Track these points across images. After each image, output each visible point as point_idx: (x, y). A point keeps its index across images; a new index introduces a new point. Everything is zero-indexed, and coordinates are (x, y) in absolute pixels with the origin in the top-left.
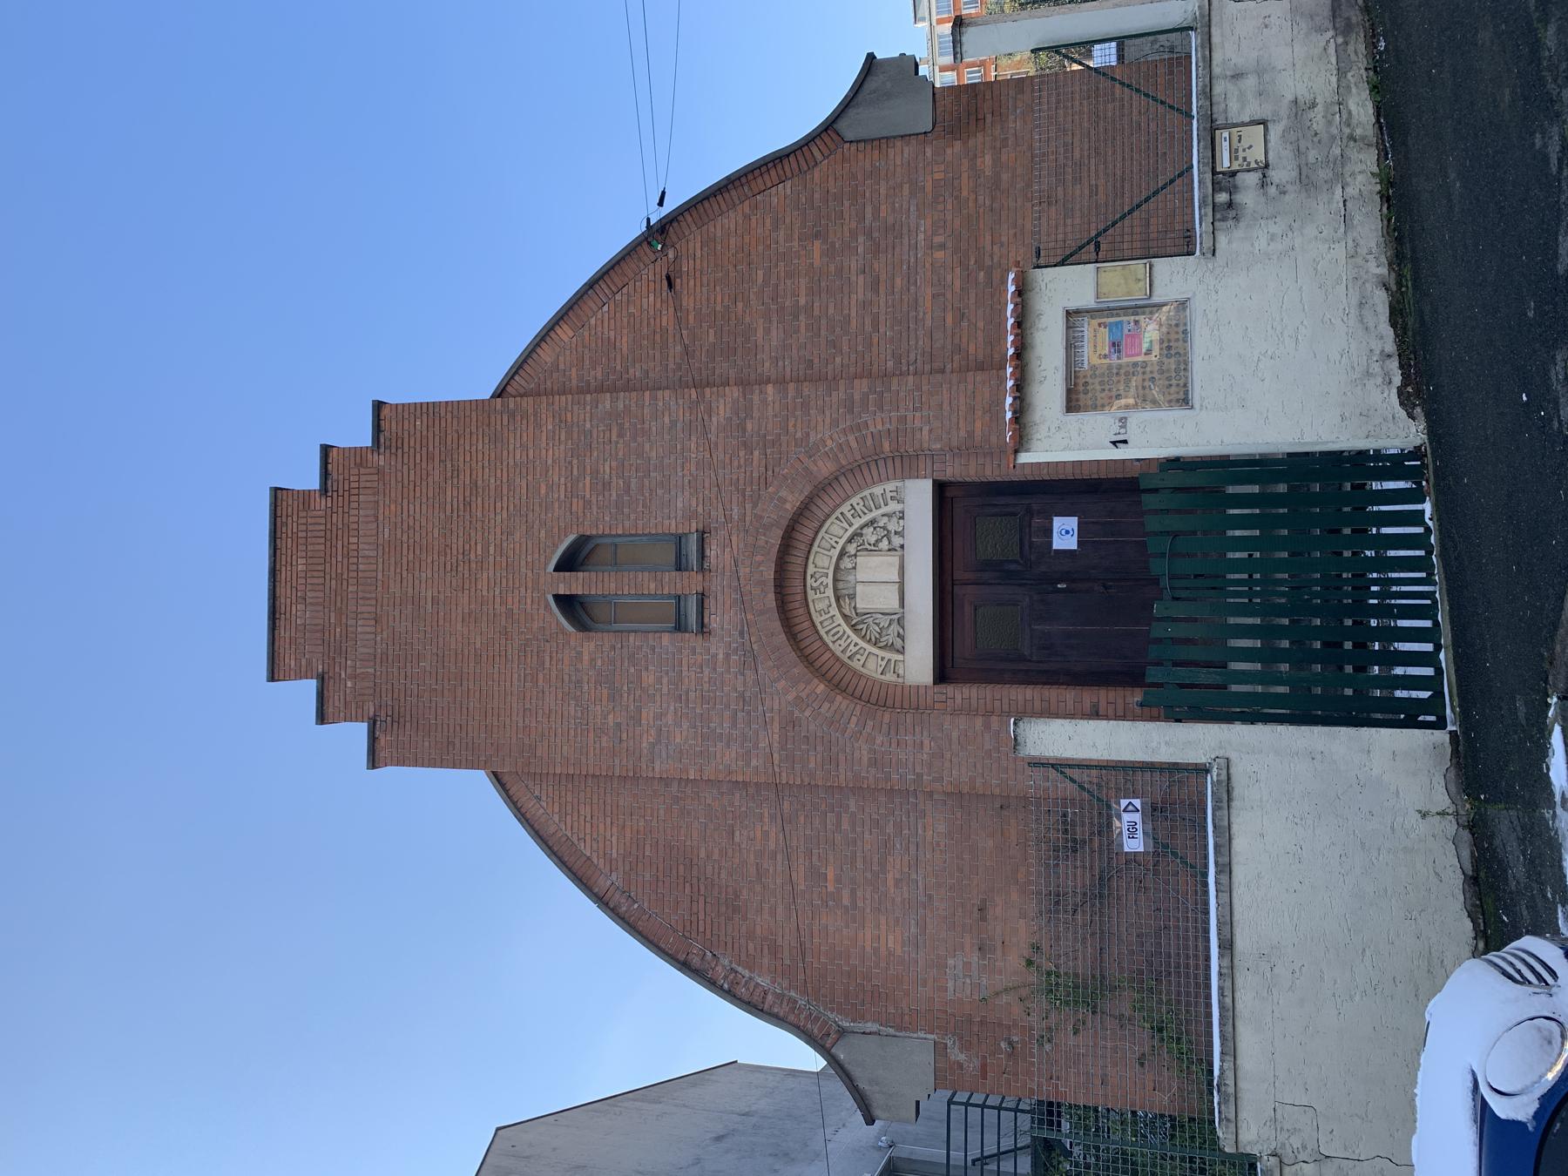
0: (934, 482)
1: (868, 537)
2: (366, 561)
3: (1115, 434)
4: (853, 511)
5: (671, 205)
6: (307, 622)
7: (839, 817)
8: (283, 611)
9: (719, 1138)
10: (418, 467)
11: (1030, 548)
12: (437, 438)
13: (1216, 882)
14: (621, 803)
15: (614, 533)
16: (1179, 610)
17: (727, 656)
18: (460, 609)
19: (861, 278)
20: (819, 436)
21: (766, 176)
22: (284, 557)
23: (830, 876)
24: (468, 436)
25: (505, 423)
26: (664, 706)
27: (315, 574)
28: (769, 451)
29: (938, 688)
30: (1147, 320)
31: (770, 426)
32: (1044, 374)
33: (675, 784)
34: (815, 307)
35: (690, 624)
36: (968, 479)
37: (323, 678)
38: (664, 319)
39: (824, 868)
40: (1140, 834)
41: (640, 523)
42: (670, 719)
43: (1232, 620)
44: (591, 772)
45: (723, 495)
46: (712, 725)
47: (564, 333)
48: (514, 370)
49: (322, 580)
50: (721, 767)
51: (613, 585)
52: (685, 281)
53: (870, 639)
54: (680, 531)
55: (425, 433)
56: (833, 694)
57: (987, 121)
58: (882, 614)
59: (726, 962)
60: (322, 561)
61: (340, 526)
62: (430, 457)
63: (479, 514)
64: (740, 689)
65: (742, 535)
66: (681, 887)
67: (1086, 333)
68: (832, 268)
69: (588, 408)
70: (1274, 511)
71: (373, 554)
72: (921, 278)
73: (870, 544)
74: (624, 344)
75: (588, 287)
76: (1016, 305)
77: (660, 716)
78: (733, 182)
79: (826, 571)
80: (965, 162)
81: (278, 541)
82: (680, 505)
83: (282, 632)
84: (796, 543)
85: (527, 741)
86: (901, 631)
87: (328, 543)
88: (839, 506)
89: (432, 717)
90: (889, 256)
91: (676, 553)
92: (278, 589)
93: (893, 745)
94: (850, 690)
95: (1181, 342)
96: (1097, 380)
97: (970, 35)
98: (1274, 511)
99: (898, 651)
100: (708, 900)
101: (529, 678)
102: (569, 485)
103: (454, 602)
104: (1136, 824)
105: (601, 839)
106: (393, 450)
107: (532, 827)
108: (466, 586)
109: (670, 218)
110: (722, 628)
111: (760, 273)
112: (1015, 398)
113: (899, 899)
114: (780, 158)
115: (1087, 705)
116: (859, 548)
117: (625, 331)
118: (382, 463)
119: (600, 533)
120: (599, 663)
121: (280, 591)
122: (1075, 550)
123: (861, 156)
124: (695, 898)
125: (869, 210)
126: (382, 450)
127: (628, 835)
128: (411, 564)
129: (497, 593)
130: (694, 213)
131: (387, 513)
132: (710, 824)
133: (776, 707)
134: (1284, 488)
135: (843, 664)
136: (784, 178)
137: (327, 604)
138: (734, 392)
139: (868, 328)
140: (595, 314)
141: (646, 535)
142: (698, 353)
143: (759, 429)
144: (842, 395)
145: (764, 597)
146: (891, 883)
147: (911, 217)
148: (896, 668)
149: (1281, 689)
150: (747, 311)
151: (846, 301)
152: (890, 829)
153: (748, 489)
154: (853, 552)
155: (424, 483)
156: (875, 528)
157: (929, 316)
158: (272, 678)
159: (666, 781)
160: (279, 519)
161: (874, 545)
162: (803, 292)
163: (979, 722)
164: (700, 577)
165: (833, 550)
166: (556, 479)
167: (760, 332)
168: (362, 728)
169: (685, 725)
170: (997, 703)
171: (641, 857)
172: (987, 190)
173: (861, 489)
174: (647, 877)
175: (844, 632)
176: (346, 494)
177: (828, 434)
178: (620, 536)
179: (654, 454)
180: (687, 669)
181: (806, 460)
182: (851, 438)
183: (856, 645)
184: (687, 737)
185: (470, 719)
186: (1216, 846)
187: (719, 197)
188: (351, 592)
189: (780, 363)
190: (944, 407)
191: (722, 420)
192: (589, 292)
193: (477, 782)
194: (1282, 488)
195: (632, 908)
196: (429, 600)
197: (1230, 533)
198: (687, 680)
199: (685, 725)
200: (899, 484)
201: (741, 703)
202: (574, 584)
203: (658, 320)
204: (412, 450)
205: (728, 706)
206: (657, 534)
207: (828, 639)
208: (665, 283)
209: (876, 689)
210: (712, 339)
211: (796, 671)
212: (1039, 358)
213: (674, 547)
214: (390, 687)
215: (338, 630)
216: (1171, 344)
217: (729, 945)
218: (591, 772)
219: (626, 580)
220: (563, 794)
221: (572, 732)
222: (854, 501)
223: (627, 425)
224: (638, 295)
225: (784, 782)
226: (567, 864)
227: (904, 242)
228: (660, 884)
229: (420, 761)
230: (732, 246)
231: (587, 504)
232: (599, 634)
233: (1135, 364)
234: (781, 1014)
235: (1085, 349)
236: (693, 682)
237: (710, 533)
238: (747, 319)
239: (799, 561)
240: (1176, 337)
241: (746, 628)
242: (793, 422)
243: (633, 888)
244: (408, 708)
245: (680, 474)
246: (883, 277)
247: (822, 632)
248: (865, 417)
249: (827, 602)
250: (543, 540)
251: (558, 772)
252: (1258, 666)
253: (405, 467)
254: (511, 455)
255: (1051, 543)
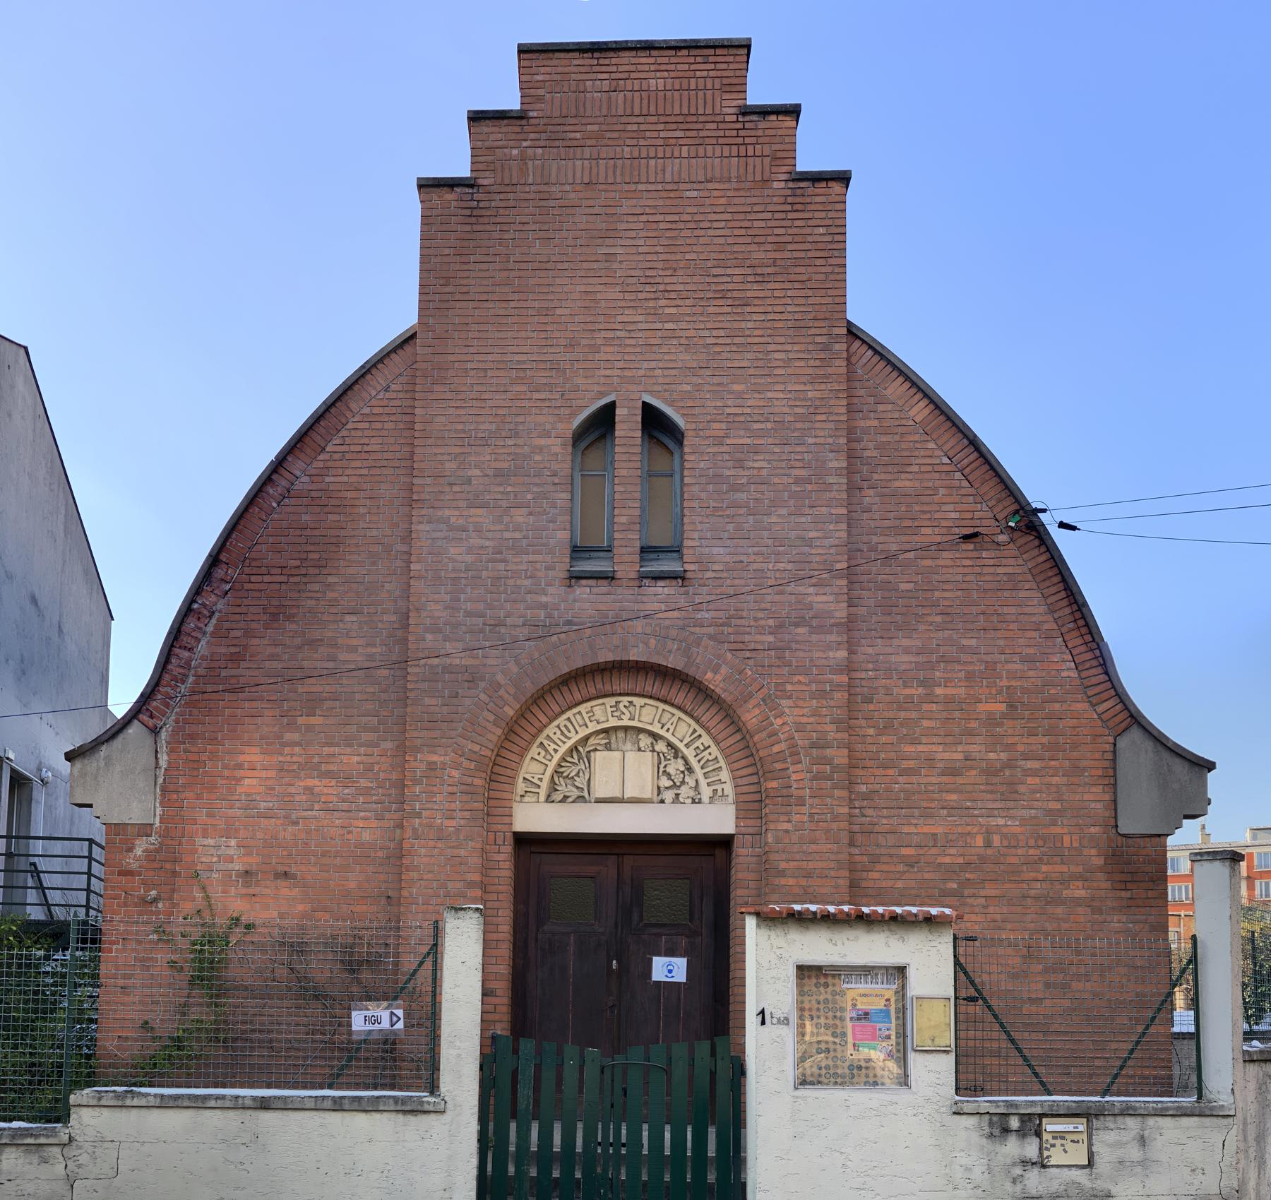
0: (732, 836)
1: (673, 765)
2: (660, 167)
3: (771, 1014)
4: (702, 748)
5: (1058, 536)
6: (588, 95)
7: (375, 730)
8: (602, 61)
9: (34, 600)
10: (769, 231)
11: (654, 934)
12: (802, 254)
13: (324, 1097)
14: (383, 486)
15: (686, 473)
16: (591, 1072)
17: (544, 606)
18: (600, 288)
19: (960, 756)
20: (787, 710)
21: (1083, 648)
22: (666, 60)
23: (313, 720)
24: (802, 293)
25: (818, 339)
26: (490, 535)
27: (645, 102)
28: (772, 653)
29: (509, 835)
30: (890, 1048)
31: (801, 654)
32: (839, 943)
33: (404, 548)
34: (932, 705)
35: (580, 563)
36: (733, 871)
37: (522, 118)
38: (929, 531)
39: (321, 714)
40: (370, 1027)
41: (696, 504)
42: (475, 541)
43: (580, 1125)
44: (418, 450)
45: (725, 601)
46: (469, 590)
47: (920, 410)
48: (879, 348)
49: (637, 112)
50: (424, 599)
51: (624, 472)
52: (970, 554)
53: (562, 766)
54: (685, 551)
55: (810, 239)
56: (503, 725)
57: (1123, 892)
58: (589, 779)
59: (219, 606)
60: (661, 111)
61: (702, 134)
62: (779, 247)
63: (711, 309)
64: (508, 621)
65: (680, 623)
66: (296, 555)
67: (879, 986)
68: (973, 724)
69: (831, 440)
70: (689, 1169)
71: (668, 178)
72: (955, 821)
73: (665, 766)
74: (904, 483)
75: (971, 438)
76: (916, 915)
77: (478, 530)
78: (1080, 610)
79: (637, 717)
80: (1080, 869)
81: (685, 52)
82: (715, 550)
83: (578, 60)
84: (668, 683)
85: (451, 373)
86: (570, 800)
87: (681, 119)
88: (708, 731)
89: (478, 258)
90: (982, 787)
91: (660, 547)
92: (627, 54)
93: (450, 788)
94: (507, 745)
95: (865, 1080)
96: (830, 997)
97: (1220, 870)
98: (689, 1169)
99: (549, 796)
100: (284, 586)
101: (521, 374)
102: (742, 419)
103: (610, 280)
104: (379, 1024)
105: (344, 463)
106: (790, 200)
107: (356, 382)
108: (627, 296)
109: (1044, 537)
110: (575, 601)
111: (973, 642)
112: (815, 913)
113: (292, 790)
114: (1105, 664)
115: (491, 985)
116: (661, 755)
117: (917, 484)
118: (775, 185)
119: (686, 457)
120: (537, 458)
121: (626, 58)
122: (651, 979)
123: (1097, 756)
124: (285, 571)
125: (1035, 764)
126: (791, 185)
127: (349, 495)
128: (654, 226)
129: (619, 334)
130: (1048, 565)
131: (716, 193)
132: (362, 587)
133: (490, 662)
134: (711, 1179)
135: (535, 737)
136: (1080, 668)
137: (609, 120)
138: (841, 613)
139: (904, 764)
140: (940, 447)
141: (682, 511)
142: (887, 570)
143: (797, 642)
144: (831, 736)
145: (610, 650)
146: (310, 783)
147: (1024, 811)
148: (531, 794)
149: (511, 1170)
150: (931, 628)
151: (935, 739)
152: (363, 783)
153: (730, 630)
154: (657, 748)
155: (749, 240)
156: (683, 772)
157: (913, 830)
158: (523, 50)
159: (408, 538)
160: (711, 51)
161: (665, 771)
162: (949, 691)
163: (476, 877)
164: (634, 575)
165: (660, 725)
166: (750, 403)
167: (906, 642)
168: (464, 171)
169: (469, 559)
170: (494, 896)
171: (326, 510)
172: (1046, 892)
173: (726, 757)
174: (305, 517)
175: (569, 738)
176: (740, 140)
177: (789, 720)
178: (682, 480)
179: (774, 519)
180: (531, 560)
181: (760, 695)
182: (783, 746)
183: (556, 751)
184: (456, 561)
185: (476, 304)
186: (359, 1099)
187: (1063, 594)
188: (623, 150)
189: (870, 666)
190: (812, 846)
191: (809, 599)
192: (965, 440)
193: (405, 316)
194: (711, 1178)
195: (271, 500)
196: (612, 250)
197: (668, 1128)
198: (519, 560)
199: (469, 559)
200: (731, 799)
201: (492, 622)
202: (628, 426)
203: (928, 523)
204: (789, 223)
205: (491, 607)
206: (683, 525)
207: (561, 720)
208: (970, 531)
209: (509, 773)
210: (903, 586)
211: (528, 684)
212: (856, 939)
213: (669, 545)
214: (511, 203)
215: (578, 135)
216: (863, 1070)
217: (238, 610)
218: (418, 450)
219: (630, 488)
220: (393, 418)
221: (460, 427)
222: (714, 751)
223: (809, 487)
224: (958, 499)
225: (409, 670)
226: (317, 424)
227: (997, 803)
228: (298, 532)
229: (427, 243)
230: (1006, 610)
231: (719, 440)
232: (569, 458)
233: (844, 1035)
234: (170, 667)
235: (863, 986)
236: (515, 568)
237: (682, 586)
238: (922, 627)
239: (648, 689)
240: (871, 1075)
241: (575, 628)
242: (803, 681)
243: (293, 501)
244: (488, 227)
245: (750, 550)
246: (959, 780)
247: (569, 714)
248: (806, 761)
249: (602, 719)
250: (680, 388)
251: (417, 411)
252: (534, 1148)
253: (769, 215)
254: (779, 348)
255: (659, 955)
